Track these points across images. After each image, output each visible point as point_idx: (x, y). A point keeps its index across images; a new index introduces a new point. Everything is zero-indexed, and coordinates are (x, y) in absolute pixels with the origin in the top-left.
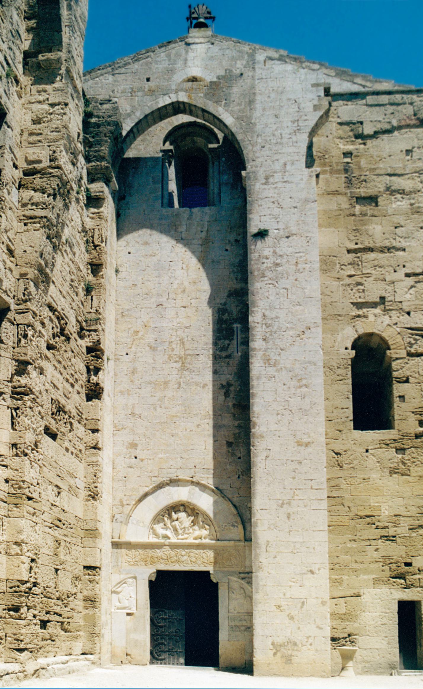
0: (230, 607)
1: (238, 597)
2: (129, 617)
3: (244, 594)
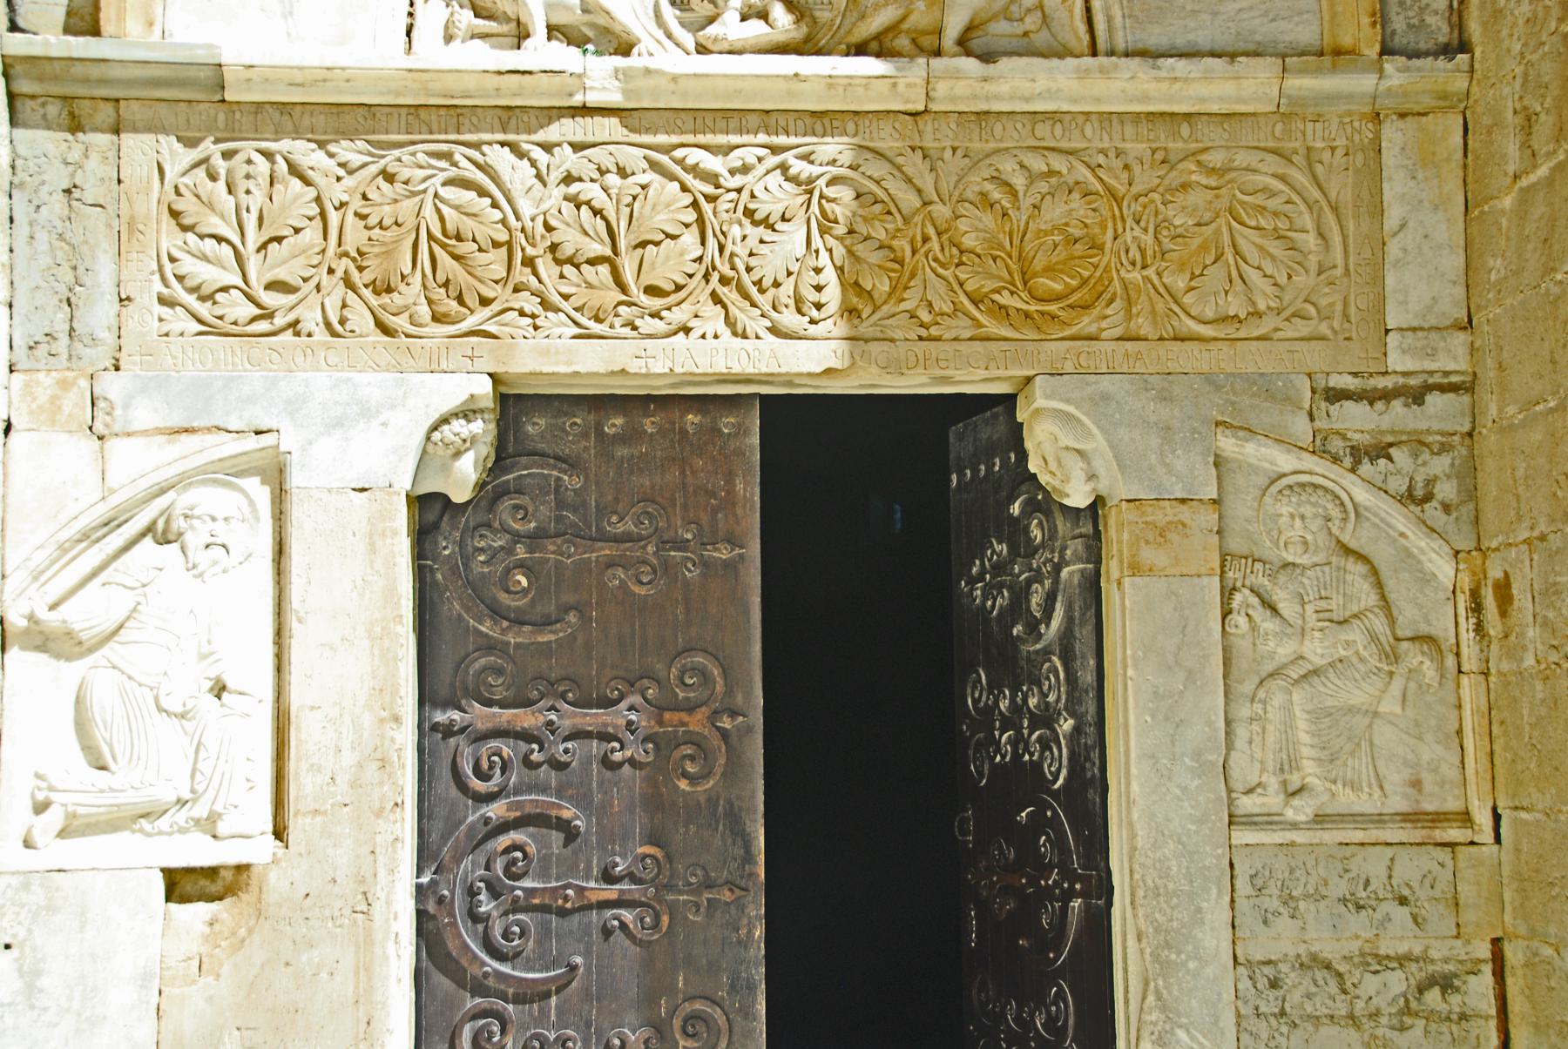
0: (1244, 769)
1: (1316, 650)
2: (196, 913)
3: (1379, 624)
